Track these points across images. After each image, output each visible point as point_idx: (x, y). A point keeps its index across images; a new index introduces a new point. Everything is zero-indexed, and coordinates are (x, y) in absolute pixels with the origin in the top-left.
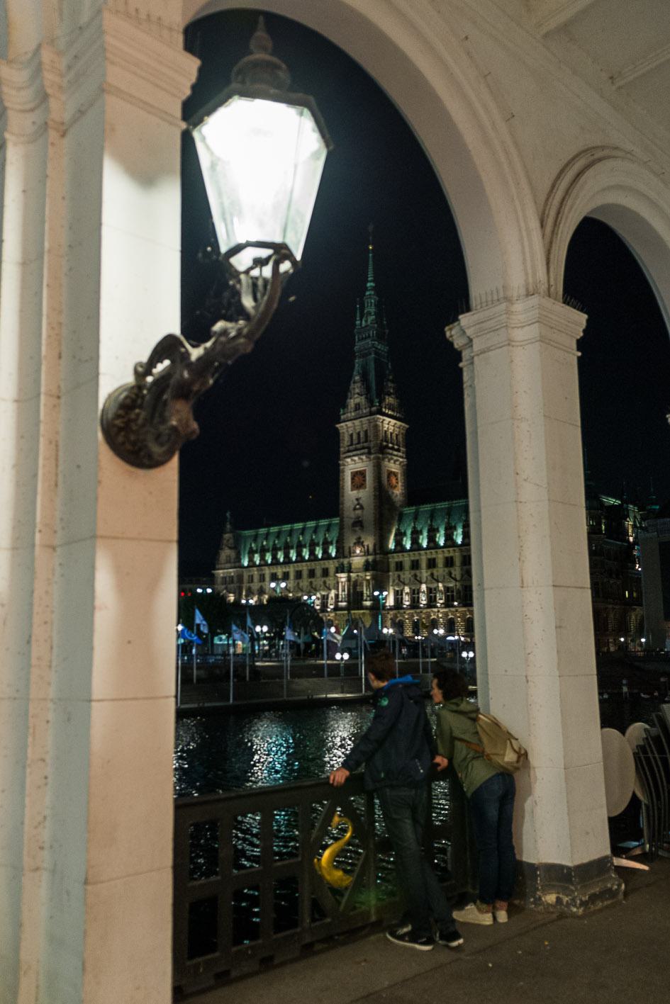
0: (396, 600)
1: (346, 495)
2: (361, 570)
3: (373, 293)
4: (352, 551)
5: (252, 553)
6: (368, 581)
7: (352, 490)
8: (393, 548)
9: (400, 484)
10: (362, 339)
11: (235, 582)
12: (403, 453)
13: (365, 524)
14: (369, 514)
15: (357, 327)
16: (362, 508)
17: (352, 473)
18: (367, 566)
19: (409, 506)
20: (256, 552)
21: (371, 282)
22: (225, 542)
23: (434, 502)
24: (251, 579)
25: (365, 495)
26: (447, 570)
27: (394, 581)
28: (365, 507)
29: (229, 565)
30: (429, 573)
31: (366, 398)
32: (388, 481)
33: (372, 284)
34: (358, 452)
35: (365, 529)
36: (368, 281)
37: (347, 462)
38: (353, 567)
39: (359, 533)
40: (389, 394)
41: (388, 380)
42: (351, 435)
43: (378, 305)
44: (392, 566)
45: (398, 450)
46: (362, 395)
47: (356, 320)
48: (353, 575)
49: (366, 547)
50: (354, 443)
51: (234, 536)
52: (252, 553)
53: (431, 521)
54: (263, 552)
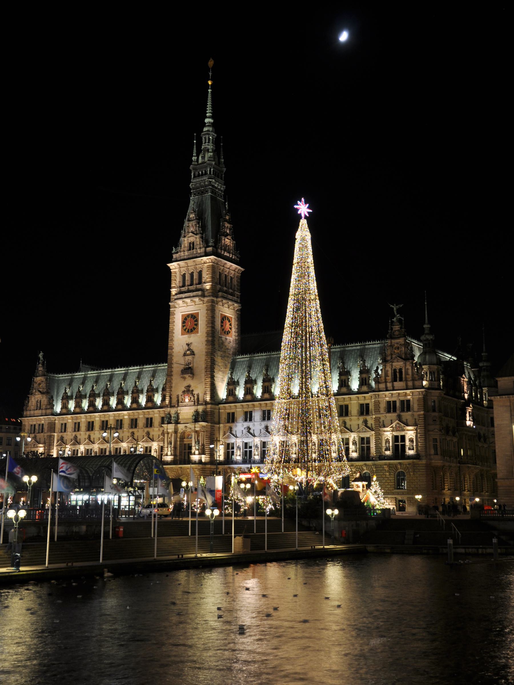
1: (175, 339)
2: (191, 420)
3: (211, 129)
4: (180, 400)
5: (66, 398)
6: (196, 432)
7: (182, 334)
8: (225, 397)
9: (233, 330)
10: (199, 175)
11: (46, 431)
12: (237, 297)
13: (196, 371)
14: (200, 362)
15: (193, 163)
16: (193, 353)
17: (183, 315)
18: (197, 418)
19: (242, 354)
20: (71, 398)
21: (209, 117)
22: (35, 385)
23: (269, 351)
24: (64, 427)
25: (198, 340)
27: (224, 434)
28: (196, 352)
29: (39, 412)
30: (263, 426)
31: (202, 237)
32: (222, 326)
33: (211, 120)
34: (191, 294)
35: (195, 377)
36: (206, 117)
37: (179, 304)
38: (180, 417)
39: (189, 381)
40: (226, 235)
41: (226, 221)
42: (184, 276)
43: (216, 142)
45: (232, 294)
46: (196, 234)
47: (193, 156)
48: (181, 427)
49: (196, 396)
50: (187, 284)
51: (46, 380)
52: (66, 398)
53: (267, 370)
54: (80, 397)
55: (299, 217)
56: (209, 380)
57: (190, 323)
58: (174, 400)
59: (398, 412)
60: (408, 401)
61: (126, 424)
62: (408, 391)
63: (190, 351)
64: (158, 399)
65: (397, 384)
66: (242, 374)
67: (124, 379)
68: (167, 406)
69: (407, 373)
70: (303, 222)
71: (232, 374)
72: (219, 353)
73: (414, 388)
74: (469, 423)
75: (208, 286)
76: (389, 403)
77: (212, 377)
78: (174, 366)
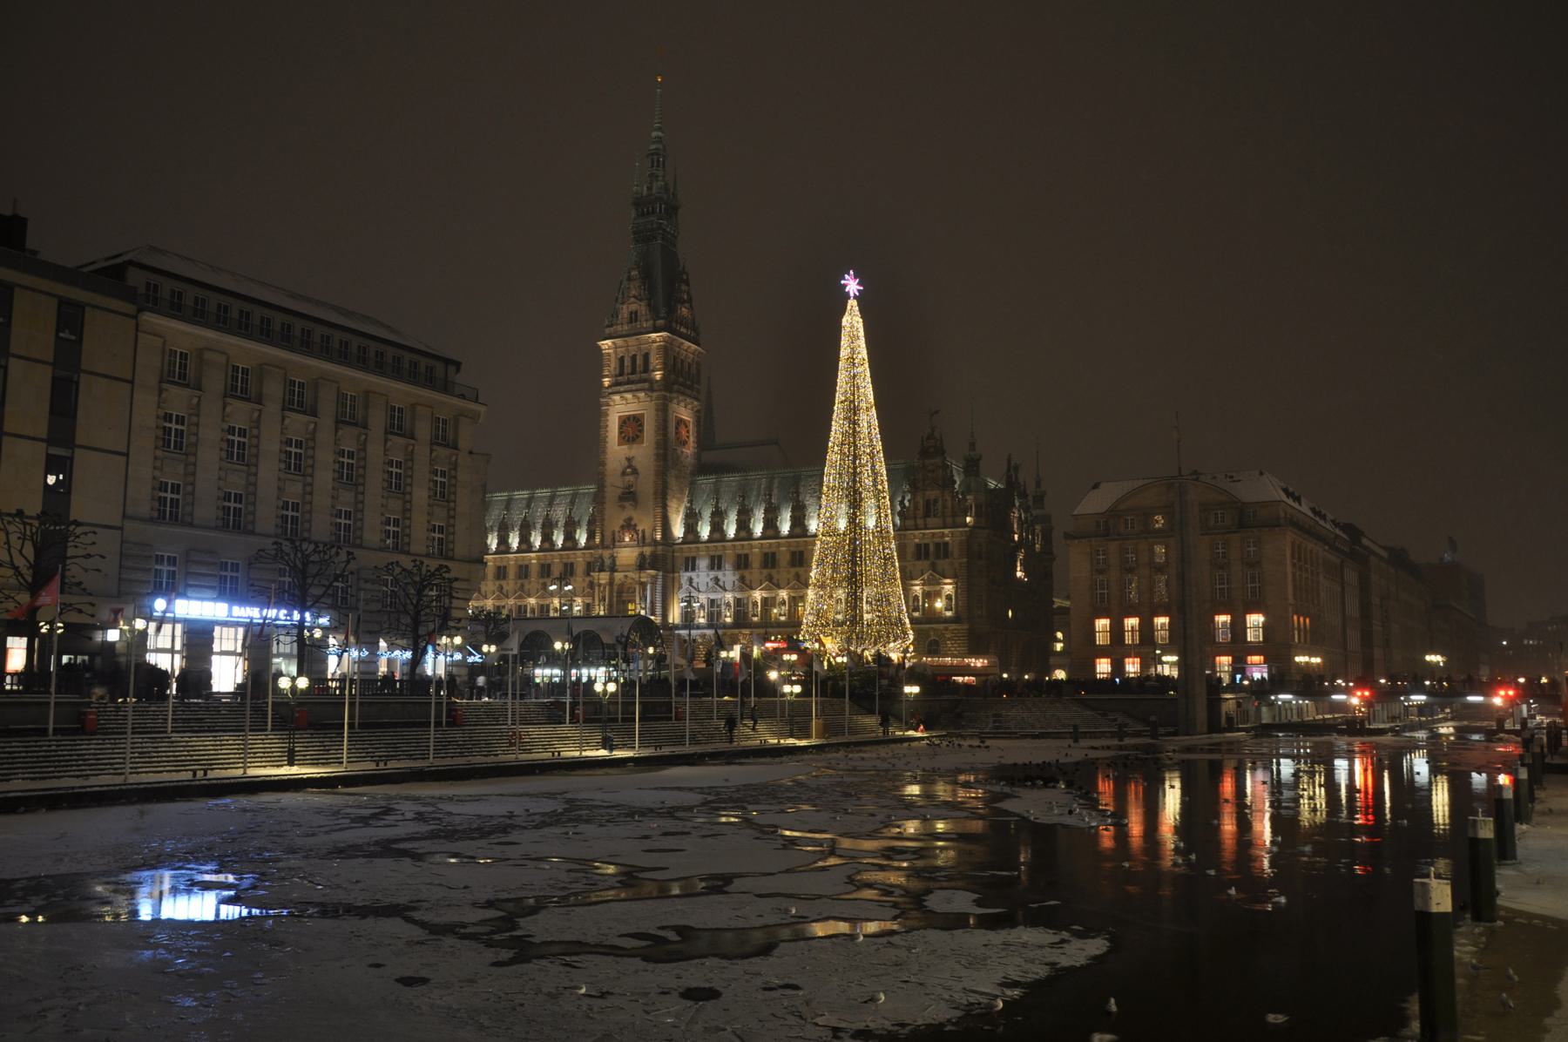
0: (711, 616)
14: (646, 484)
16: (635, 472)
18: (642, 565)
26: (765, 572)
39: (630, 512)
44: (680, 563)
48: (618, 576)
55: (847, 296)
56: (659, 510)
57: (631, 428)
58: (608, 542)
59: (932, 558)
60: (946, 544)
61: (534, 571)
62: (946, 531)
63: (631, 468)
64: (582, 538)
65: (930, 521)
66: (706, 502)
67: (528, 506)
68: (597, 547)
69: (944, 507)
70: (852, 304)
71: (691, 502)
72: (673, 472)
73: (955, 526)
74: (1019, 574)
75: (658, 375)
76: (918, 546)
77: (665, 507)
78: (609, 489)
